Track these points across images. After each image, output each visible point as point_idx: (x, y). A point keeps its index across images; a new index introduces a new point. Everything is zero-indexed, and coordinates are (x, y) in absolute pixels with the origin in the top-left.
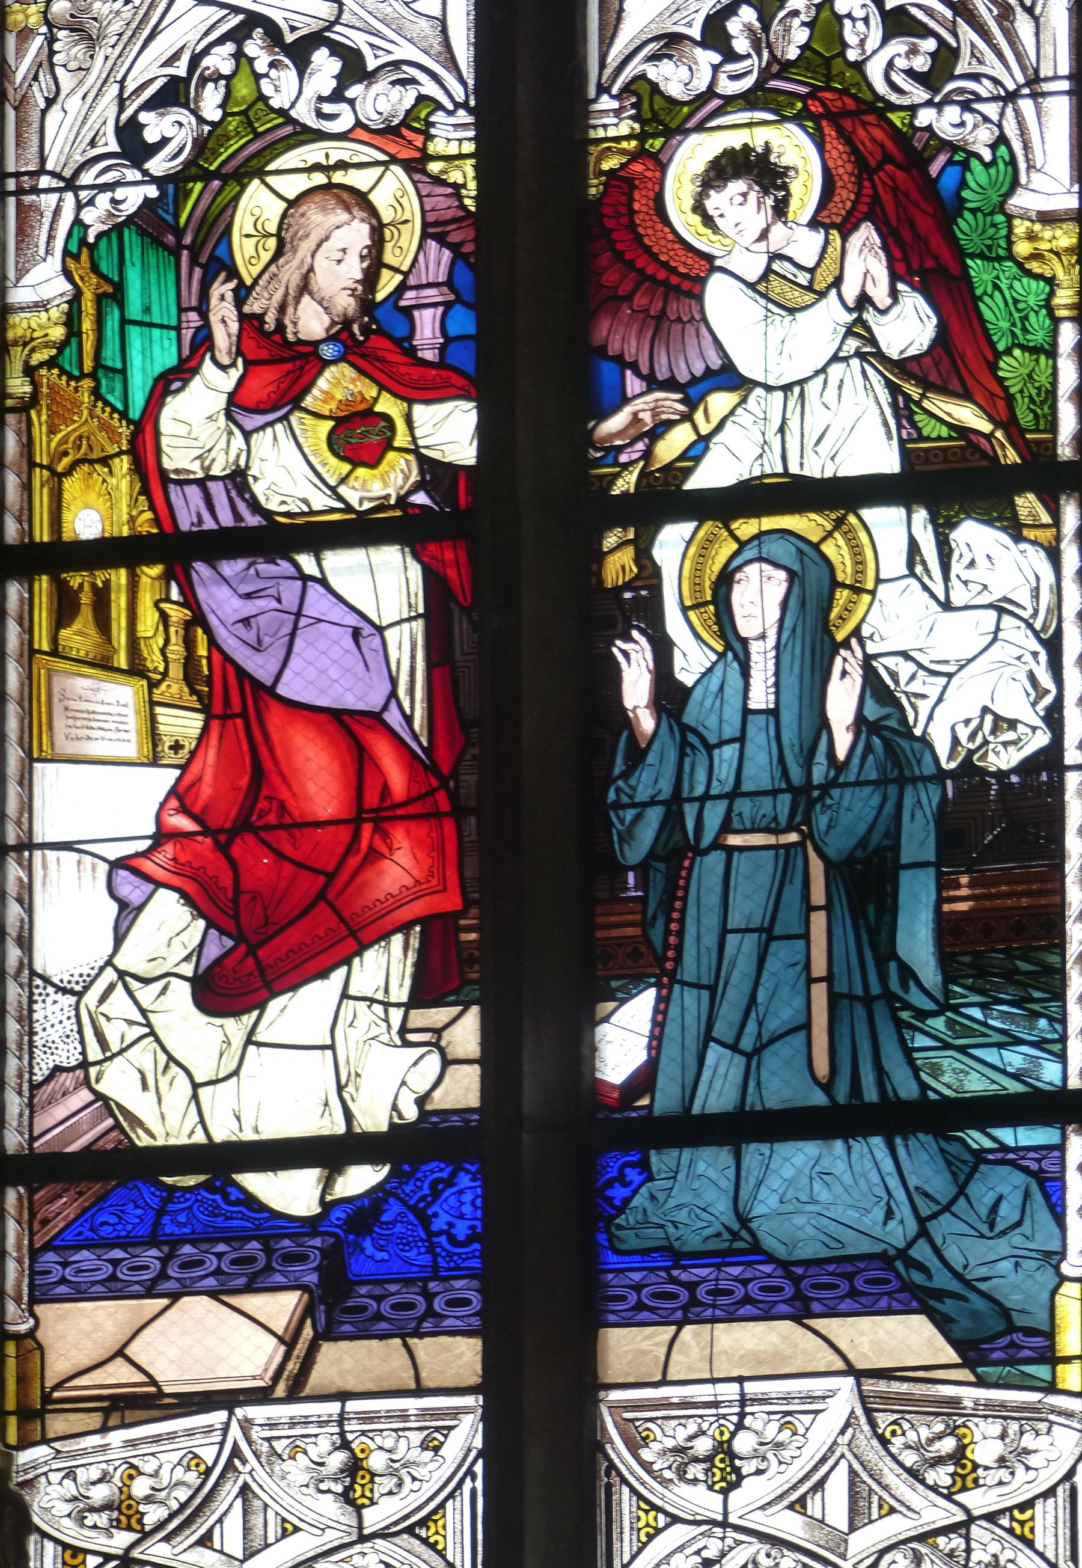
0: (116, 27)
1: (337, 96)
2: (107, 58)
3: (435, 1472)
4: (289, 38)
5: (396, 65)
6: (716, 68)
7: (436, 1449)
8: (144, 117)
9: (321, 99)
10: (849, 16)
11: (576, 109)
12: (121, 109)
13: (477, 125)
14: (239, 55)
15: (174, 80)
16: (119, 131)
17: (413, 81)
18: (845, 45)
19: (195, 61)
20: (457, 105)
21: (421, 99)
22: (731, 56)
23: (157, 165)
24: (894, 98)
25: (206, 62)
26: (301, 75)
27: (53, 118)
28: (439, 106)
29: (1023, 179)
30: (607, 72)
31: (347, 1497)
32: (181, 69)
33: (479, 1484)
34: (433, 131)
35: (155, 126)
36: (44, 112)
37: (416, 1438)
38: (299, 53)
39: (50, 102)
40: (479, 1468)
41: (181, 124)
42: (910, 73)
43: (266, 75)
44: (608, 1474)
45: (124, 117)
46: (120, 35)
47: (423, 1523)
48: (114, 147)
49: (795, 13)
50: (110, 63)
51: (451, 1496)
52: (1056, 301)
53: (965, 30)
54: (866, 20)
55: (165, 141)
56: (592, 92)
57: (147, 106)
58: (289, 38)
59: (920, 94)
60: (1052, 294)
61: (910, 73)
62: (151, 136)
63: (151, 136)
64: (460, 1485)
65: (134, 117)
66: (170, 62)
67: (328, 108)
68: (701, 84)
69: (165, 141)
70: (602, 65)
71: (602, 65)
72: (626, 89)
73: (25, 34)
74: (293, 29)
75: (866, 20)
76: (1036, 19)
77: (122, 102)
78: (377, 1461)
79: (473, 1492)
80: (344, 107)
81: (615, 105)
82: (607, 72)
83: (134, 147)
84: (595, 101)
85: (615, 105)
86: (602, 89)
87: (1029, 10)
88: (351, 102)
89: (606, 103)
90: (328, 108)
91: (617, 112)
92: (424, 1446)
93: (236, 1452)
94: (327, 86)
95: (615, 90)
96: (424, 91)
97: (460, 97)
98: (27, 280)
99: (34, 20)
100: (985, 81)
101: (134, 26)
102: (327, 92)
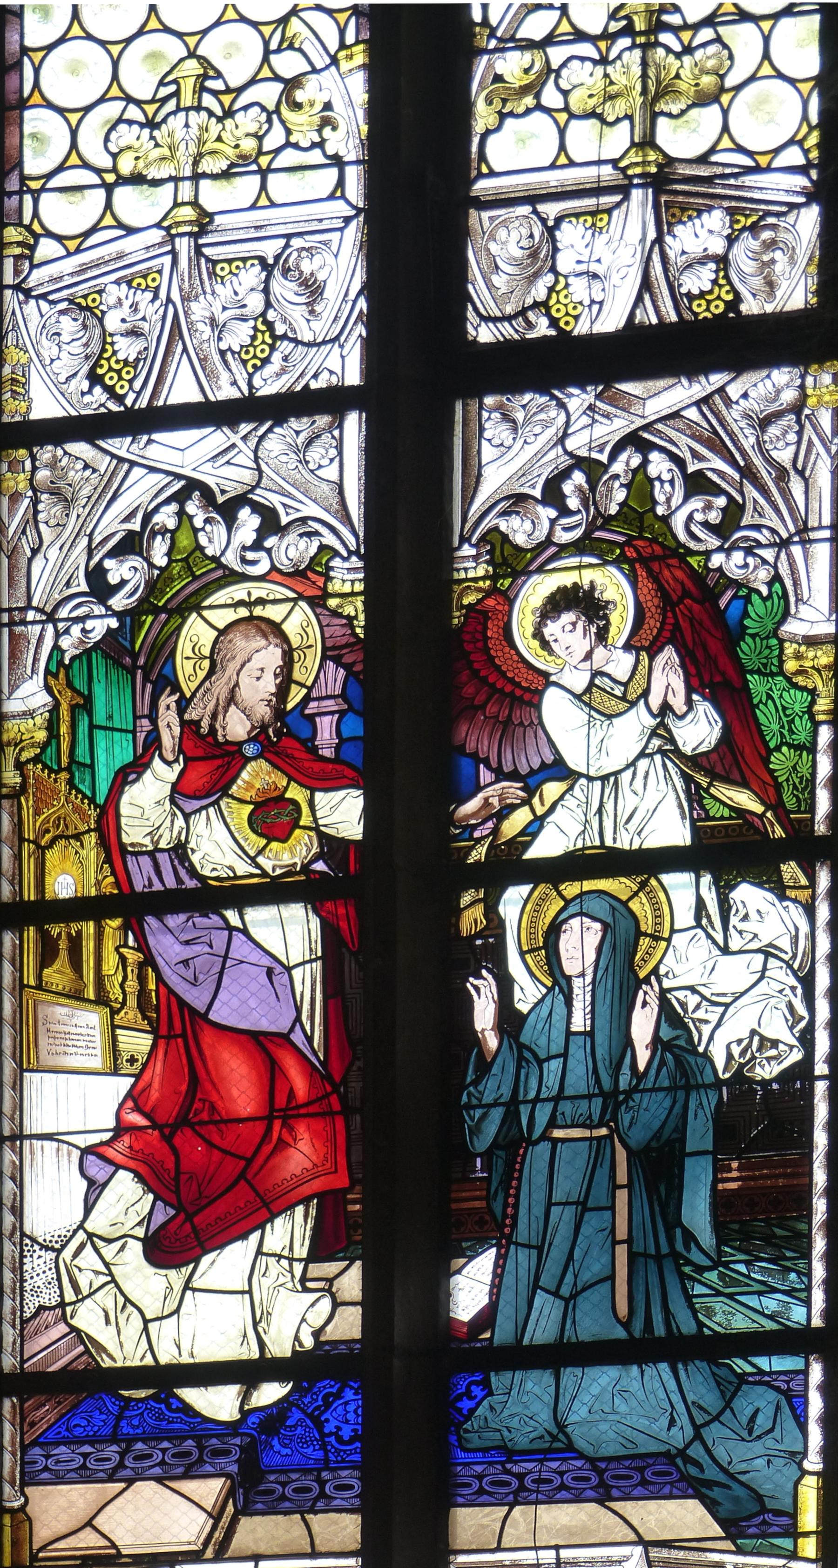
1: (257, 546)
6: (553, 522)
20: (350, 553)
23: (118, 602)
28: (337, 554)
62: (113, 579)
63: (113, 579)
67: (250, 555)
72: (483, 539)
83: (100, 587)
86: (463, 540)
88: (269, 551)
90: (250, 555)
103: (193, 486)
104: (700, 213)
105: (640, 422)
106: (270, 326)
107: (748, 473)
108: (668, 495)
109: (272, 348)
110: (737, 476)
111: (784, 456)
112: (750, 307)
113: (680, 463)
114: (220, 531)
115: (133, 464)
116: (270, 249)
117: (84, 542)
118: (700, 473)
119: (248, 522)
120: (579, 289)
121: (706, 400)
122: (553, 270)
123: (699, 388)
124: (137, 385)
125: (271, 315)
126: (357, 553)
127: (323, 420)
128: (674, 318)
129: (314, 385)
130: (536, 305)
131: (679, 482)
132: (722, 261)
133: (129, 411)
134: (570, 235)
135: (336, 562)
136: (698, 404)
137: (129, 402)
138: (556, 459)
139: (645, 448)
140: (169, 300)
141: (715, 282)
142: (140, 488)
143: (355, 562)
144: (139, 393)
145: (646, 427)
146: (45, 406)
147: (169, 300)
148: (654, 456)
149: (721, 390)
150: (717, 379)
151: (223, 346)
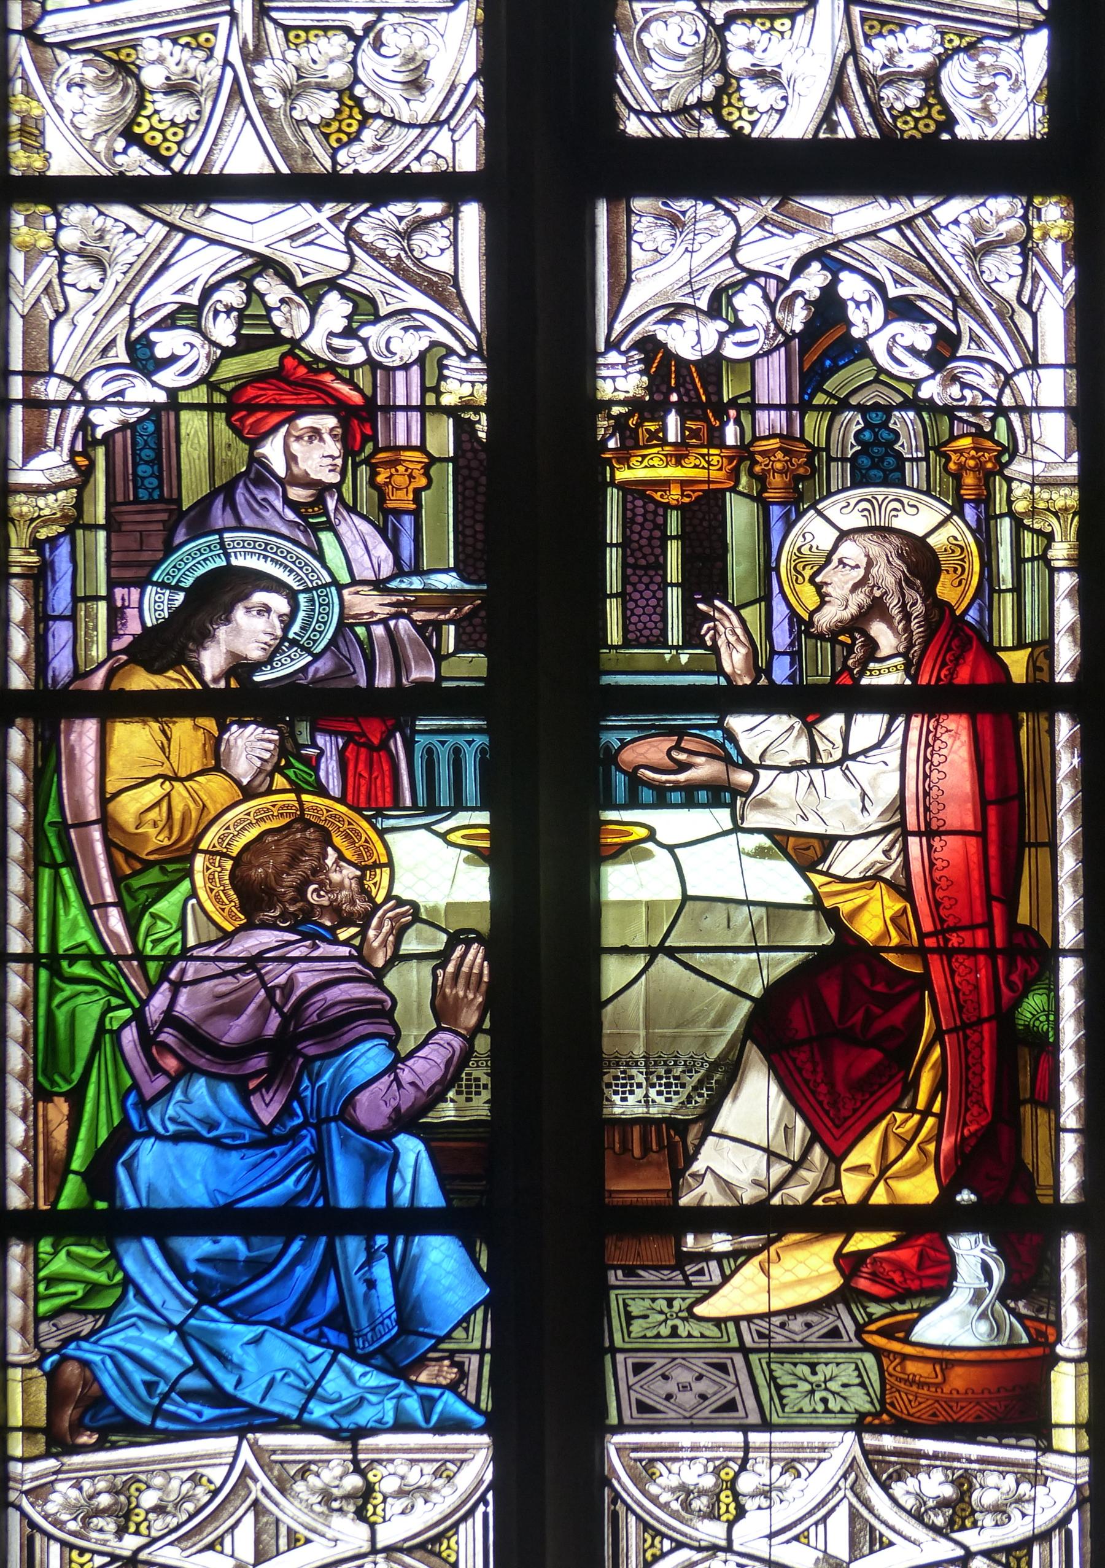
0: (129, 257)
1: (349, 332)
2: (117, 283)
3: (446, 1499)
4: (301, 281)
5: (407, 311)
6: (722, 336)
7: (450, 1478)
8: (154, 336)
9: (331, 334)
10: (852, 299)
11: (583, 361)
12: (131, 328)
13: (489, 372)
14: (250, 291)
15: (184, 307)
16: (130, 346)
17: (425, 328)
18: (850, 324)
19: (207, 293)
21: (434, 344)
22: (737, 326)
23: (168, 377)
24: (896, 370)
25: (217, 296)
26: (313, 311)
27: (62, 329)
28: (451, 352)
29: (1021, 450)
30: (618, 328)
31: (361, 1515)
32: (192, 297)
33: (490, 1509)
34: (446, 372)
35: (166, 343)
36: (53, 323)
37: (429, 1468)
38: (312, 296)
39: (59, 315)
40: (490, 1496)
41: (192, 346)
42: (912, 350)
43: (278, 309)
44: (614, 1502)
45: (135, 334)
46: (131, 264)
47: (438, 1539)
48: (124, 358)
49: (801, 294)
50: (121, 288)
51: (463, 1519)
52: (1051, 554)
53: (967, 322)
54: (869, 303)
55: (174, 359)
56: (601, 347)
57: (157, 327)
58: (301, 281)
59: (922, 369)
60: (1048, 547)
61: (912, 350)
62: (161, 352)
63: (161, 352)
64: (471, 1512)
65: (145, 334)
66: (182, 290)
67: (338, 343)
68: (709, 345)
69: (174, 359)
70: (610, 328)
71: (610, 328)
72: (637, 345)
73: (33, 257)
74: (305, 274)
75: (869, 303)
76: (1034, 316)
77: (132, 321)
78: (389, 1485)
79: (485, 1515)
80: (354, 343)
81: (623, 360)
82: (618, 328)
83: (143, 359)
84: (602, 354)
85: (623, 360)
86: (612, 345)
87: (1028, 307)
88: (365, 342)
89: (613, 357)
90: (338, 343)
91: (625, 366)
92: (437, 1474)
93: (246, 1472)
94: (339, 325)
95: (623, 348)
96: (435, 337)
97: (471, 340)
98: (35, 463)
99: (44, 242)
100: (988, 366)
101: (144, 257)
102: (338, 329)
103: (265, 264)
104: (903, 27)
105: (829, 239)
106: (358, 102)
107: (962, 301)
108: (865, 320)
109: (362, 125)
110: (949, 304)
111: (1008, 289)
112: (967, 130)
113: (880, 286)
114: (302, 317)
115: (189, 234)
116: (358, 22)
117: (124, 311)
118: (904, 299)
119: (335, 311)
120: (752, 92)
121: (909, 222)
122: (723, 68)
123: (899, 210)
124: (188, 147)
125: (359, 91)
126: (479, 353)
127: (431, 208)
128: (874, 133)
129: (416, 167)
130: (700, 104)
131: (879, 307)
132: (931, 77)
133: (178, 176)
134: (738, 34)
135: (453, 361)
136: (897, 226)
137: (177, 164)
138: (725, 272)
139: (835, 268)
140: (227, 63)
141: (923, 101)
142: (198, 264)
143: (476, 362)
144: (191, 157)
145: (837, 245)
146: (65, 158)
147: (227, 63)
148: (844, 275)
149: (926, 213)
150: (921, 203)
151: (296, 114)
